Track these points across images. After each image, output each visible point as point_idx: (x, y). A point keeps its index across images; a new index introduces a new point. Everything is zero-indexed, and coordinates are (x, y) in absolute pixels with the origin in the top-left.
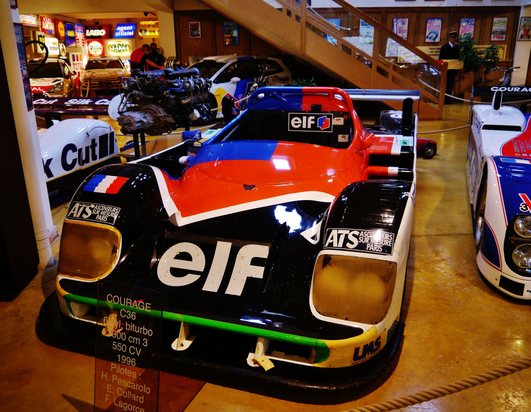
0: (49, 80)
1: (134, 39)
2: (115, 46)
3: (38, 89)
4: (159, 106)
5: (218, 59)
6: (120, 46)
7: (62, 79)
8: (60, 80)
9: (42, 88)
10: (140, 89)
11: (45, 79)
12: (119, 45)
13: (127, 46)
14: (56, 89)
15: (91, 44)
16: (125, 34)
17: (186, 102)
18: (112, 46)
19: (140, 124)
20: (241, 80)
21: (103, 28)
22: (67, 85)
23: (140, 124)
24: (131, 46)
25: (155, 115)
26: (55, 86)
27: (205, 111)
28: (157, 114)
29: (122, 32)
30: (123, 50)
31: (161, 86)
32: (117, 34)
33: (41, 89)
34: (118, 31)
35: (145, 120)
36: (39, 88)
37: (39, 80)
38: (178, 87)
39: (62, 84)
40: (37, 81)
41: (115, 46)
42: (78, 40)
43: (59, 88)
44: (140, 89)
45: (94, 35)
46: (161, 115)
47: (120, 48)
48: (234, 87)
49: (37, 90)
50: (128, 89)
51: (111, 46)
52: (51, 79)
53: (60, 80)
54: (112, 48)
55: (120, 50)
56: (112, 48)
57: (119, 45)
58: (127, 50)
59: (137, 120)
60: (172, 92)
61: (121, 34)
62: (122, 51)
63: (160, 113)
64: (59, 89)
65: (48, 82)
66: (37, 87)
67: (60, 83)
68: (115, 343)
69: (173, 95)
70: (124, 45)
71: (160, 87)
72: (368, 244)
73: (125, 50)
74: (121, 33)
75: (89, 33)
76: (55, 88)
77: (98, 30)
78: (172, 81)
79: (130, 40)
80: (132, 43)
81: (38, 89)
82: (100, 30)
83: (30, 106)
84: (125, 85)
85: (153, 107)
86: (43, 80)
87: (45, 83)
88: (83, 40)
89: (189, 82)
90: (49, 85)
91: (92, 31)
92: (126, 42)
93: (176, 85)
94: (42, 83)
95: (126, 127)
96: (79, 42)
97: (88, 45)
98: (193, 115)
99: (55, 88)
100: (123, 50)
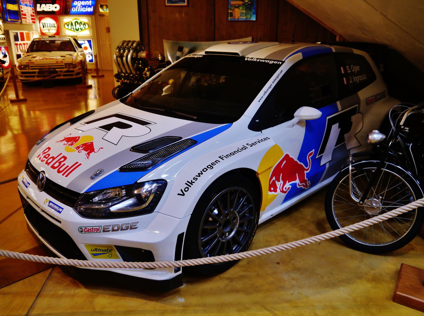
1: (94, 16)
2: (72, 24)
6: (78, 24)
12: (77, 23)
13: (86, 24)
15: (43, 21)
16: (83, 10)
18: (68, 24)
21: (57, 2)
24: (90, 24)
29: (79, 8)
30: (81, 29)
32: (74, 9)
34: (75, 7)
41: (72, 24)
42: (25, 15)
45: (46, 10)
47: (78, 26)
51: (66, 24)
54: (68, 26)
55: (77, 29)
56: (68, 26)
57: (77, 23)
58: (85, 29)
61: (79, 10)
62: (80, 30)
70: (83, 23)
73: (83, 29)
74: (78, 9)
75: (40, 8)
77: (51, 5)
79: (90, 18)
80: (92, 20)
82: (53, 4)
88: (32, 16)
91: (43, 5)
92: (84, 19)
96: (26, 18)
97: (40, 23)
100: (81, 29)
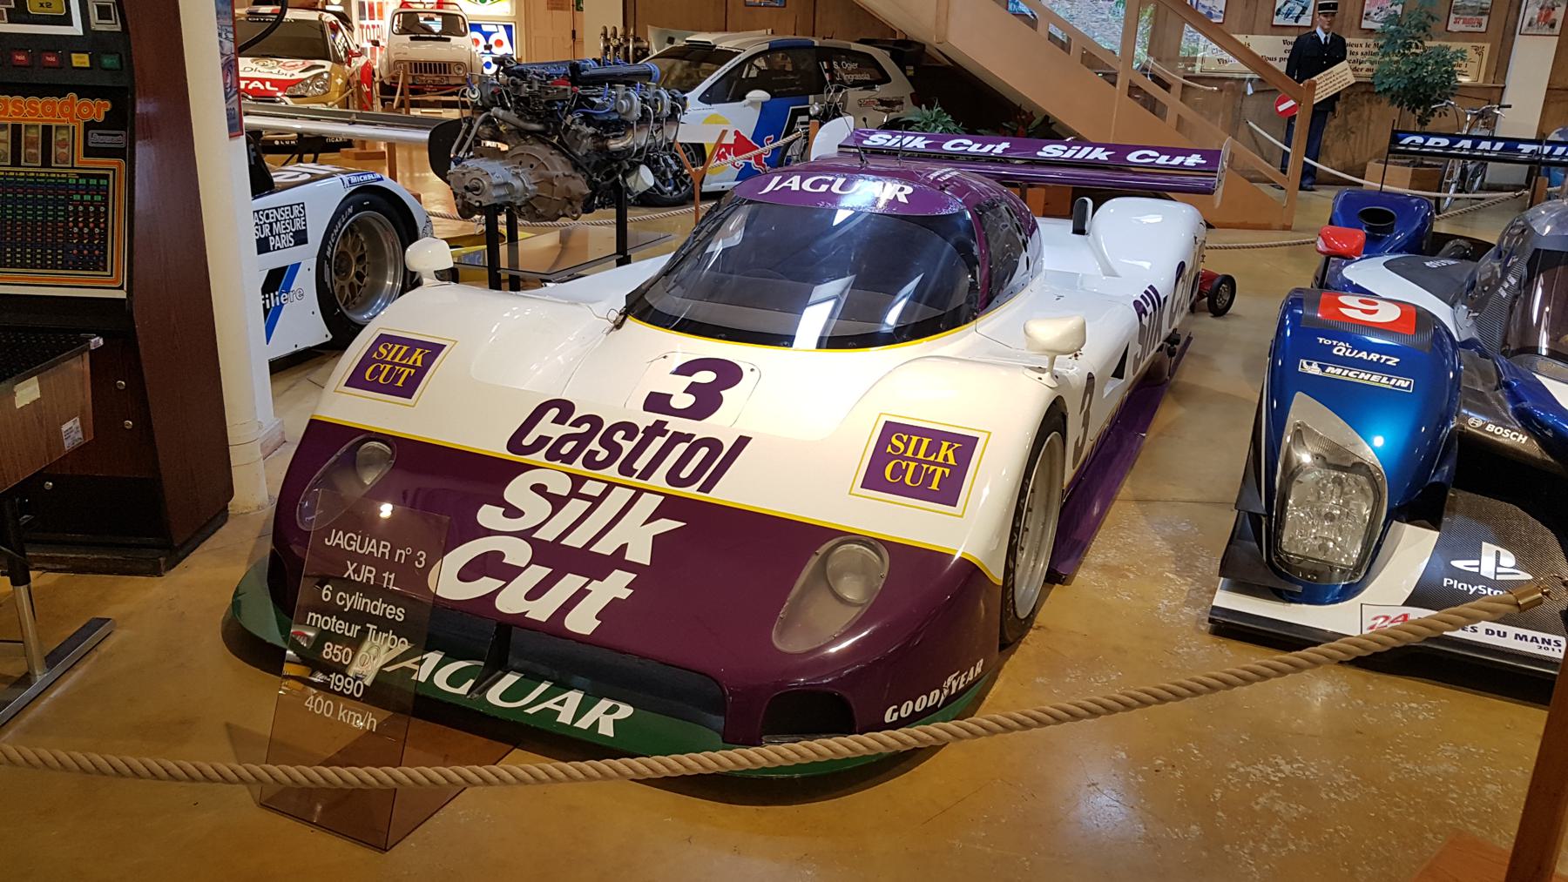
0: (293, 64)
3: (264, 85)
4: (553, 152)
5: (721, 40)
7: (328, 65)
8: (323, 67)
9: (274, 82)
10: (509, 105)
11: (285, 60)
14: (311, 88)
17: (621, 145)
19: (502, 192)
20: (772, 98)
22: (339, 81)
23: (502, 192)
25: (543, 171)
26: (309, 82)
27: (671, 171)
28: (547, 169)
31: (560, 101)
33: (271, 86)
35: (517, 183)
36: (268, 84)
37: (270, 62)
38: (603, 106)
39: (326, 76)
40: (264, 65)
43: (317, 86)
44: (509, 105)
46: (556, 173)
48: (754, 115)
49: (262, 87)
50: (480, 104)
52: (300, 62)
53: (323, 67)
59: (495, 180)
60: (588, 120)
63: (555, 169)
64: (318, 90)
65: (290, 69)
66: (263, 81)
67: (322, 73)
68: (338, 649)
69: (588, 126)
71: (556, 105)
72: (271, 238)
76: (307, 85)
78: (588, 92)
81: (264, 85)
83: (235, 127)
84: (474, 93)
85: (539, 150)
86: (278, 62)
87: (282, 71)
89: (627, 97)
90: (293, 78)
93: (597, 101)
94: (275, 71)
95: (469, 195)
98: (637, 177)
99: (307, 85)
